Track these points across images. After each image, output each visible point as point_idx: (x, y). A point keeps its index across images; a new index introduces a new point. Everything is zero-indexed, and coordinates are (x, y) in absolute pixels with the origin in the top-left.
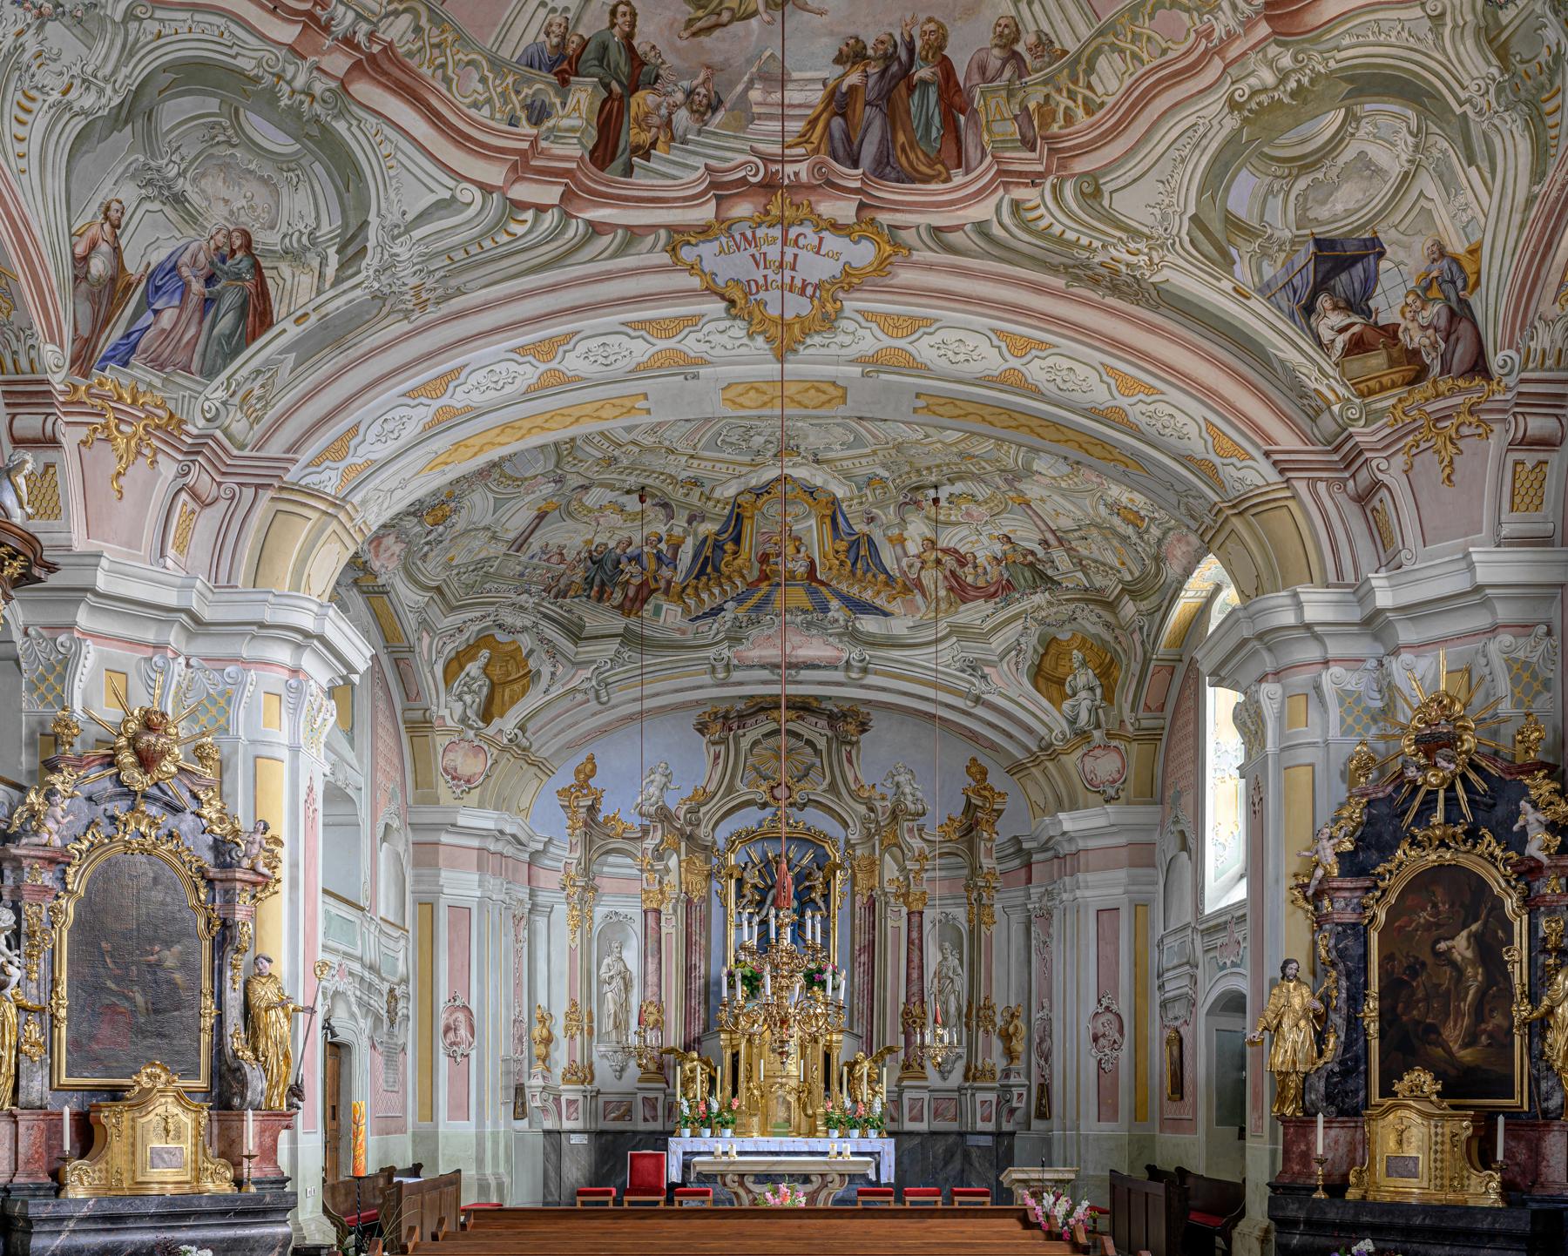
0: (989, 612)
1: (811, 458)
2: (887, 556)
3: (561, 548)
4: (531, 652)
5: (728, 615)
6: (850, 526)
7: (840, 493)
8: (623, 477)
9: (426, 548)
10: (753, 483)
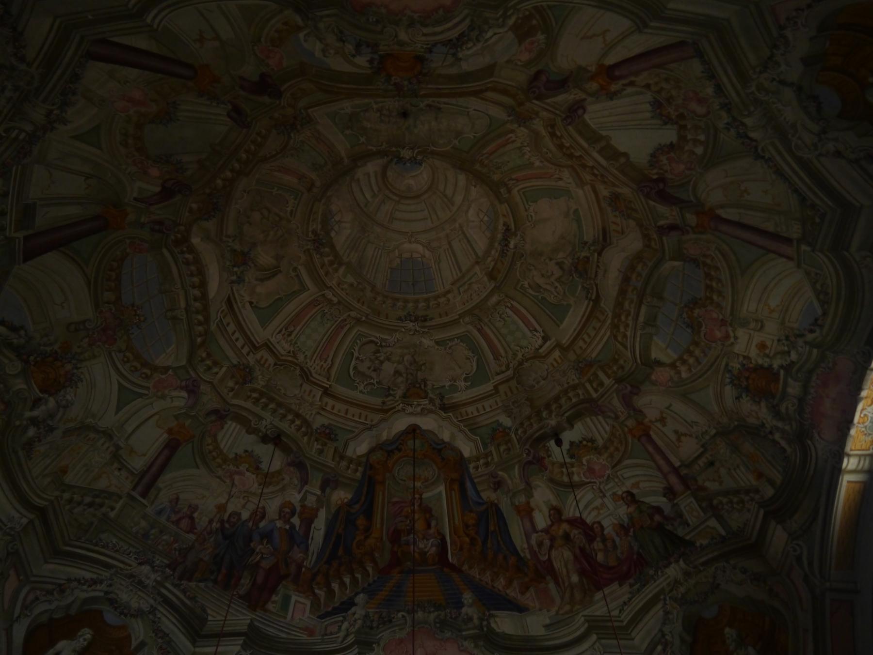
0: (625, 598)
1: (438, 402)
2: (516, 530)
3: (193, 508)
4: (142, 645)
5: (358, 612)
6: (478, 493)
7: (467, 450)
8: (257, 410)
9: (31, 432)
10: (384, 436)
